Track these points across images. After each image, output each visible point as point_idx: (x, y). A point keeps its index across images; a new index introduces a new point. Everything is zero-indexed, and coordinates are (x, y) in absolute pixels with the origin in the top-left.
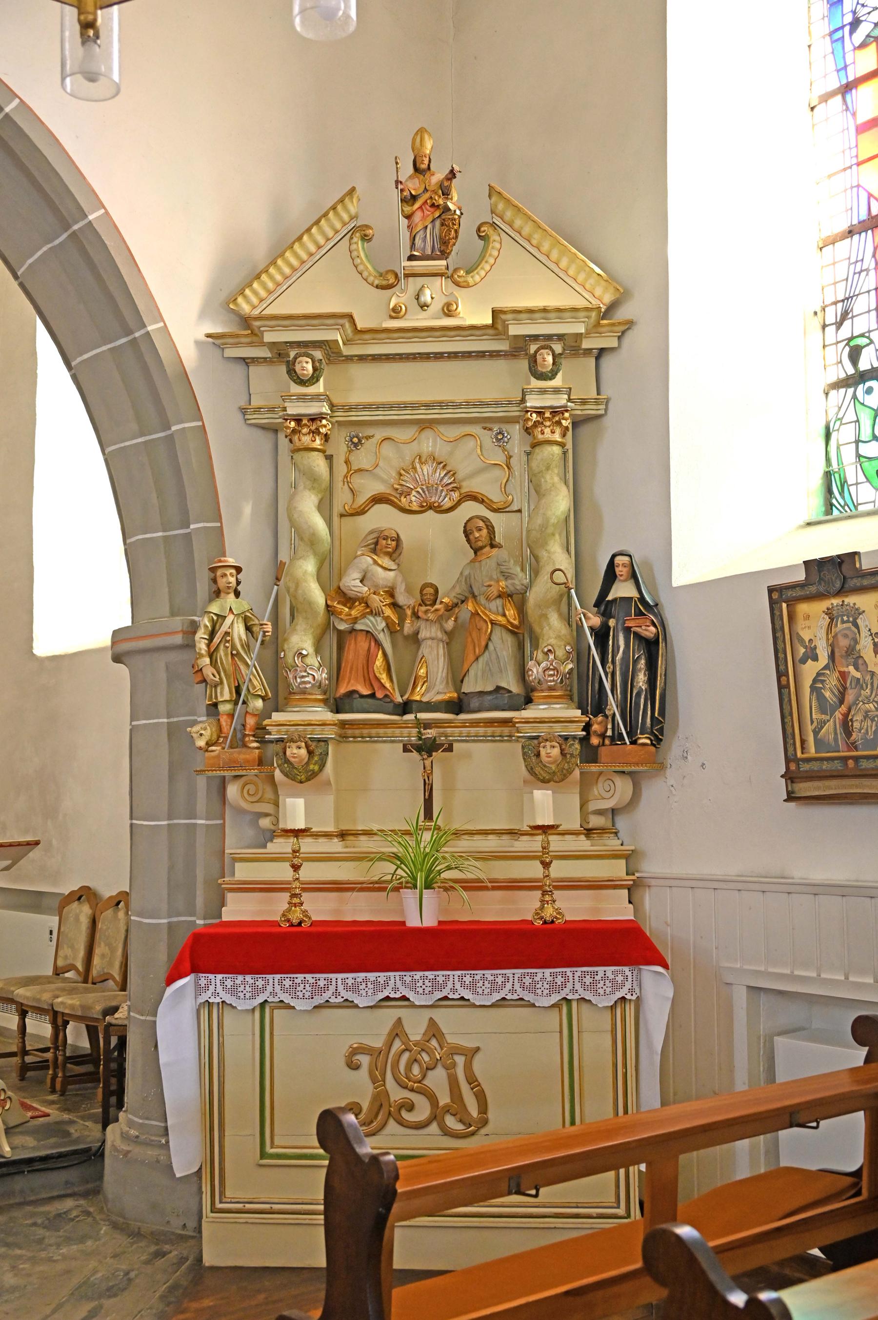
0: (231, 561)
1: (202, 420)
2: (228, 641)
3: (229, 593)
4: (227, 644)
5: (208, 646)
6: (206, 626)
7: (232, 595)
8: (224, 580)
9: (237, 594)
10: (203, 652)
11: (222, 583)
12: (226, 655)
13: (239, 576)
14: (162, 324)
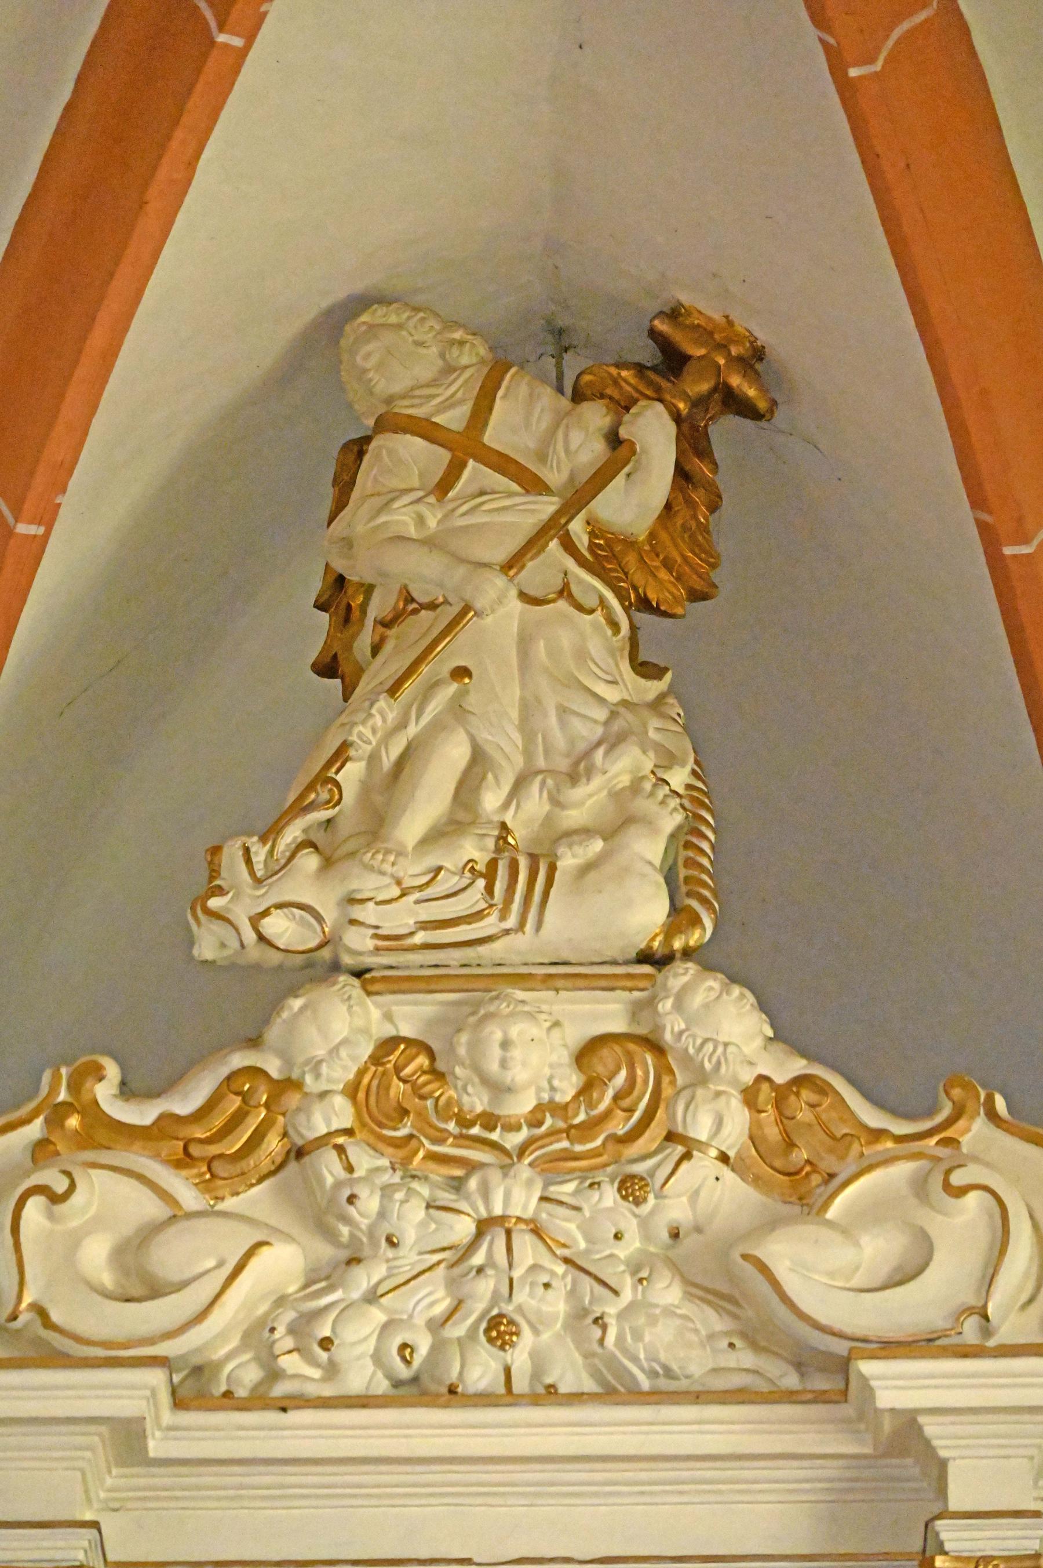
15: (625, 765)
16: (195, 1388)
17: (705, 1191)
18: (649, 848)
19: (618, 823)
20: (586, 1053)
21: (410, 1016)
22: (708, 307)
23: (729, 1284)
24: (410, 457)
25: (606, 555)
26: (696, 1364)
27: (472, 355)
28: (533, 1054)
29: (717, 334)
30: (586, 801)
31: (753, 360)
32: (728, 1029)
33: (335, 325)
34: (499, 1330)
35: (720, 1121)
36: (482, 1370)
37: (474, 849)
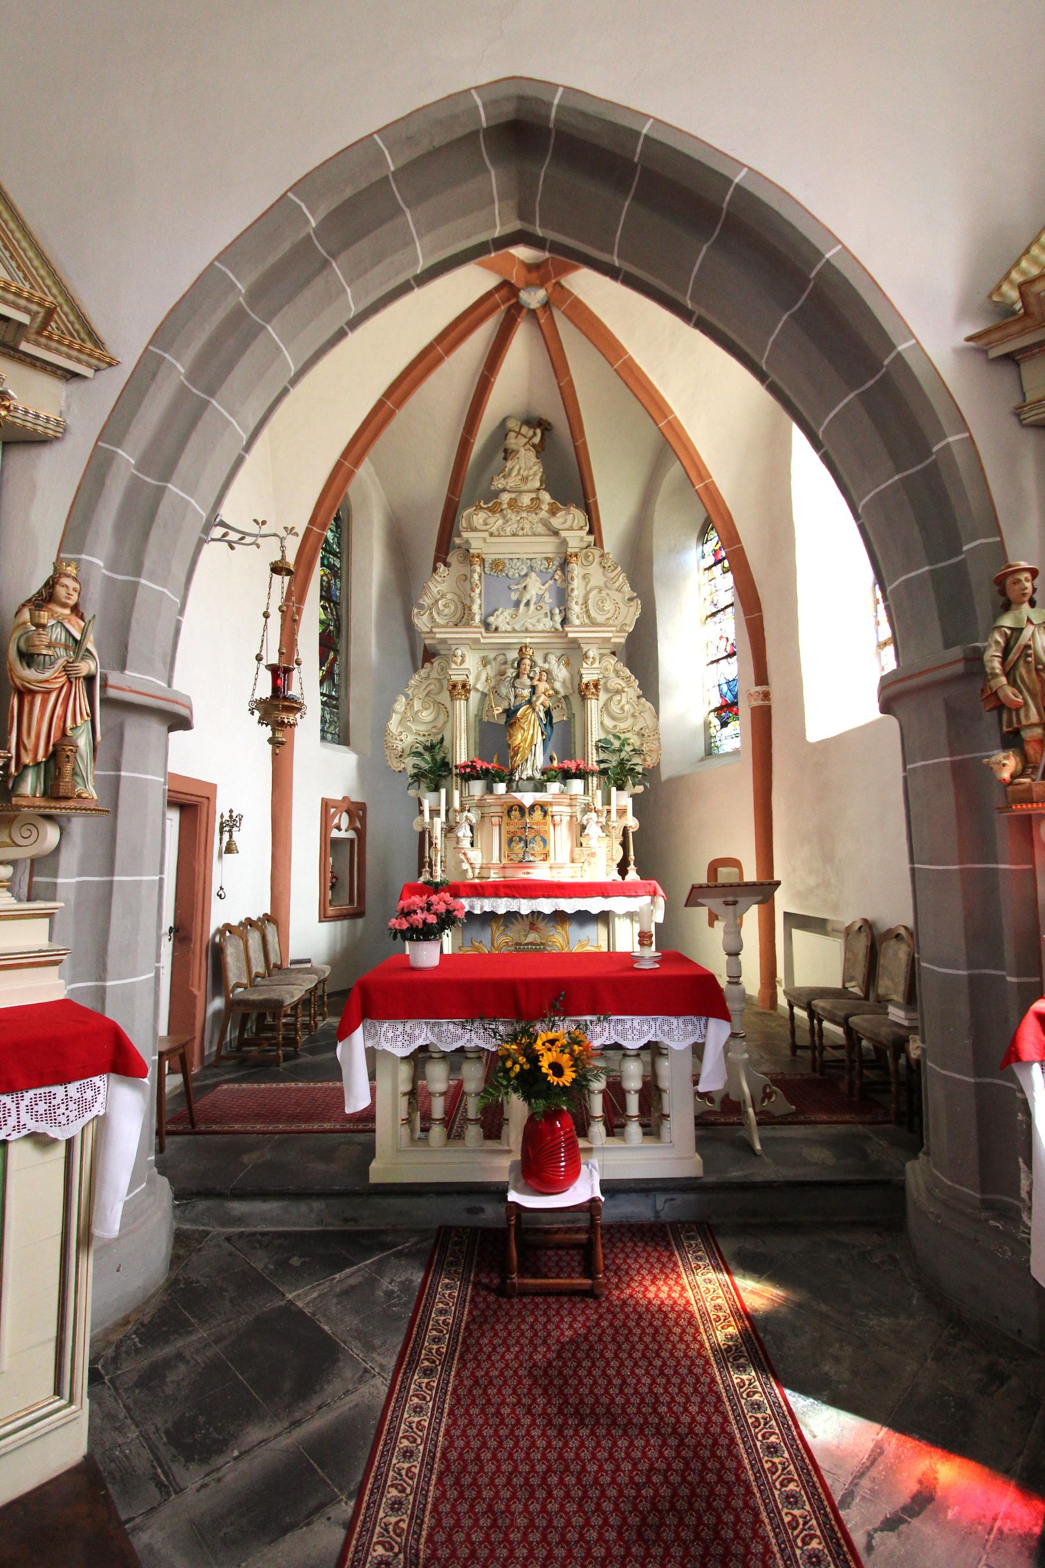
0: (1023, 564)
1: (968, 430)
2: (1030, 656)
3: (1023, 603)
4: (1030, 659)
5: (1003, 664)
6: (997, 642)
7: (1026, 606)
8: (1017, 587)
9: (1032, 603)
10: (998, 671)
11: (1012, 592)
12: (1029, 672)
13: (1036, 582)
14: (913, 341)
15: (536, 468)
16: (491, 535)
17: (543, 514)
18: (538, 477)
19: (535, 475)
20: (532, 500)
21: (513, 495)
22: (544, 417)
23: (546, 524)
24: (512, 434)
25: (534, 446)
26: (542, 532)
27: (519, 423)
28: (526, 500)
29: (545, 421)
30: (532, 472)
31: (549, 424)
32: (546, 497)
33: (504, 421)
34: (522, 529)
35: (545, 507)
36: (521, 533)
37: (520, 477)
